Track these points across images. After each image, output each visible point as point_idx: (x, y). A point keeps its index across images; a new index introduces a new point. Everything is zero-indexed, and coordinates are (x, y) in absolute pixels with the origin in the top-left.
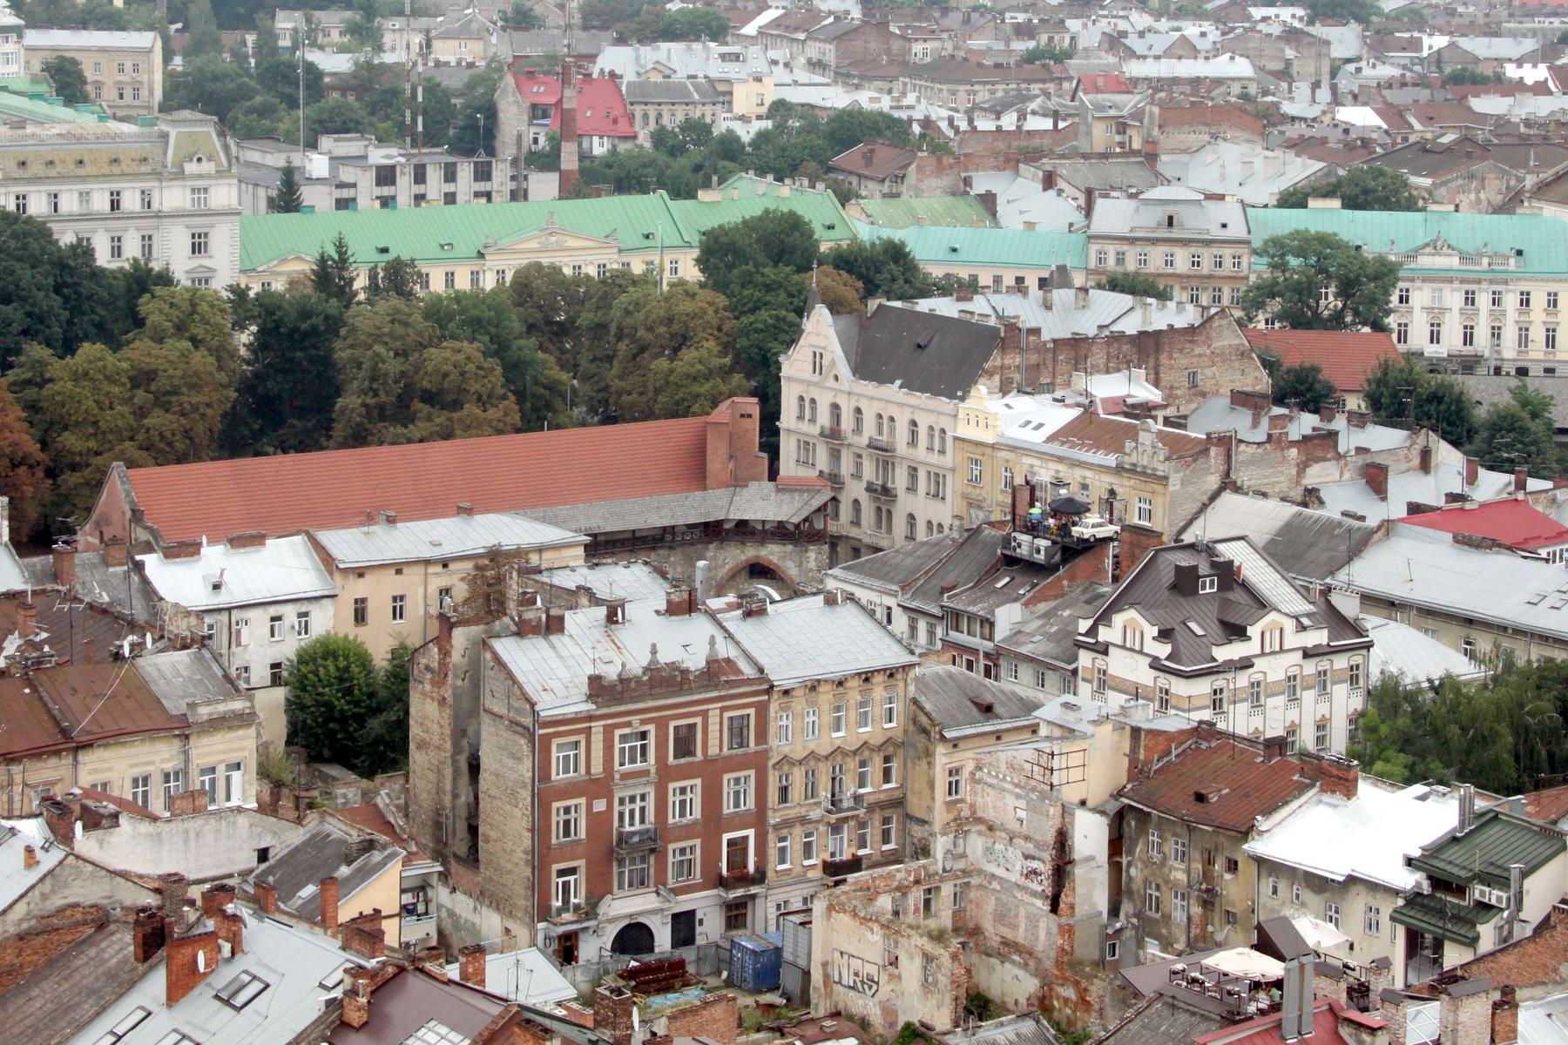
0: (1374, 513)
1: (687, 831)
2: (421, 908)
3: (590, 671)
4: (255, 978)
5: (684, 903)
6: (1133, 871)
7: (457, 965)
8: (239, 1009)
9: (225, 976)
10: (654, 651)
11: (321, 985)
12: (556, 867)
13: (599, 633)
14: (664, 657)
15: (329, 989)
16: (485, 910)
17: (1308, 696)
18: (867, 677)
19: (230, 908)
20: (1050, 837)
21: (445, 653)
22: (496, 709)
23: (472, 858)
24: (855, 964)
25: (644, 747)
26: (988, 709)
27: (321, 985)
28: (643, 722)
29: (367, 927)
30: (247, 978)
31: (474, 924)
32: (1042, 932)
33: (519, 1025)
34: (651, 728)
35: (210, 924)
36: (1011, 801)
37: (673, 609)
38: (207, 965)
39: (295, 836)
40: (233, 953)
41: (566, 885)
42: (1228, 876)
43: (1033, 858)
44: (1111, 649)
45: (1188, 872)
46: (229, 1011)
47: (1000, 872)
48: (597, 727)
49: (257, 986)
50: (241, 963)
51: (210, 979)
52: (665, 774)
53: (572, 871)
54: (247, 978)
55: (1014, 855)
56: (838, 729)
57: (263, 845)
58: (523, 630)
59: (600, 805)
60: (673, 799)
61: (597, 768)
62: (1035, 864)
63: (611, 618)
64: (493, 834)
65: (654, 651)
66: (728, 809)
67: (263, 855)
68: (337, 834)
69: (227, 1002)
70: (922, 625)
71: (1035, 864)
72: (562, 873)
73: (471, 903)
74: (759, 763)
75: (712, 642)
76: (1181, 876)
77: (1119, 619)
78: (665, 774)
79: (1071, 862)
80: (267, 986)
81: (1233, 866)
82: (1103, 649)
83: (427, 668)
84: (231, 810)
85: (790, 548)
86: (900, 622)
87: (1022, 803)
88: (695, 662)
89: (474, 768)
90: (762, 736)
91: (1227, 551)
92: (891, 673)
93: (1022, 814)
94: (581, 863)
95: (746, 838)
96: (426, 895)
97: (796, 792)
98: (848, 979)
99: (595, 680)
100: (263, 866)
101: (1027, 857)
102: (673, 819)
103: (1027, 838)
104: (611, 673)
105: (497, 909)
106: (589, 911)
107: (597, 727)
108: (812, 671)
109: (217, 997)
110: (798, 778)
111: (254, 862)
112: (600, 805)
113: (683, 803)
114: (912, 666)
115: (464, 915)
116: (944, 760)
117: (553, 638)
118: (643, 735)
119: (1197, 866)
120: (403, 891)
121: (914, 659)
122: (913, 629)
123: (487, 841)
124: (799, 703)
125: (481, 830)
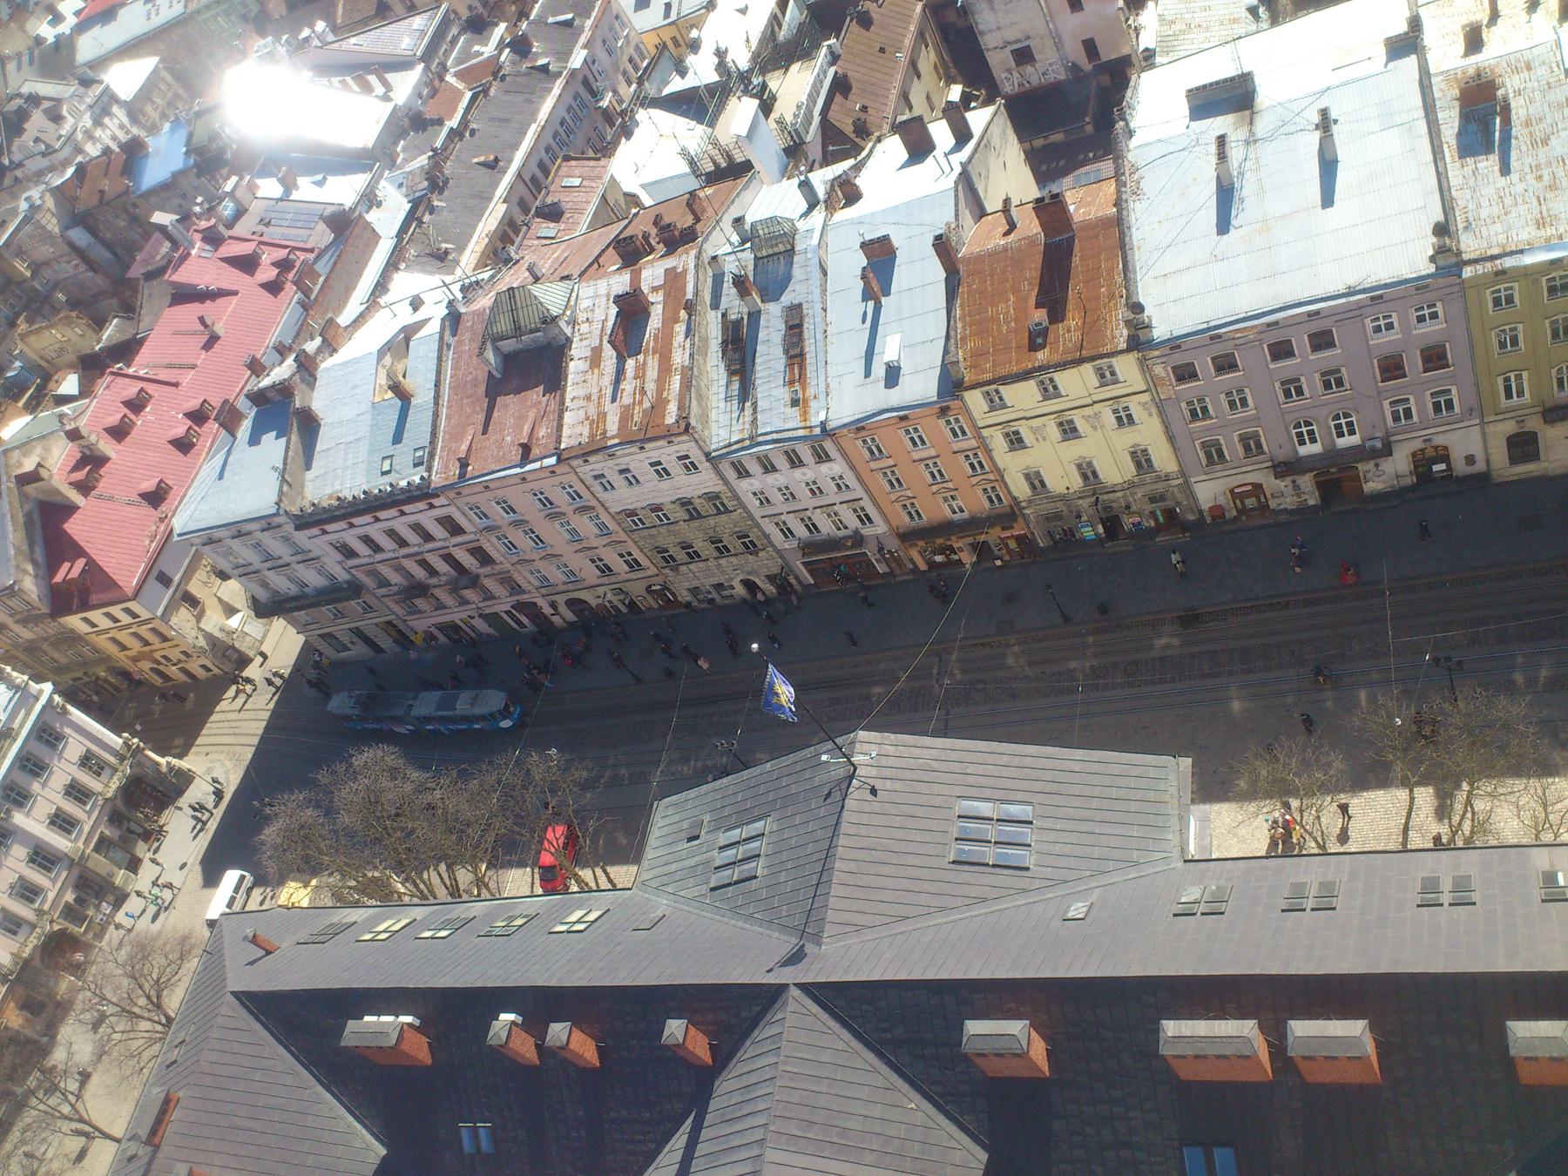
0: (65, 28)
6: (107, 236)
17: (106, 120)
20: (67, 249)
32: (101, 281)
42: (137, 210)
44: (24, 162)
45: (124, 220)
47: (66, 275)
55: (64, 265)
62: (75, 262)
71: (75, 262)
76: (122, 224)
77: (14, 148)
81: (135, 206)
82: (20, 165)
91: (25, 90)
93: (52, 250)
98: (54, 355)
103: (62, 256)
119: (124, 216)
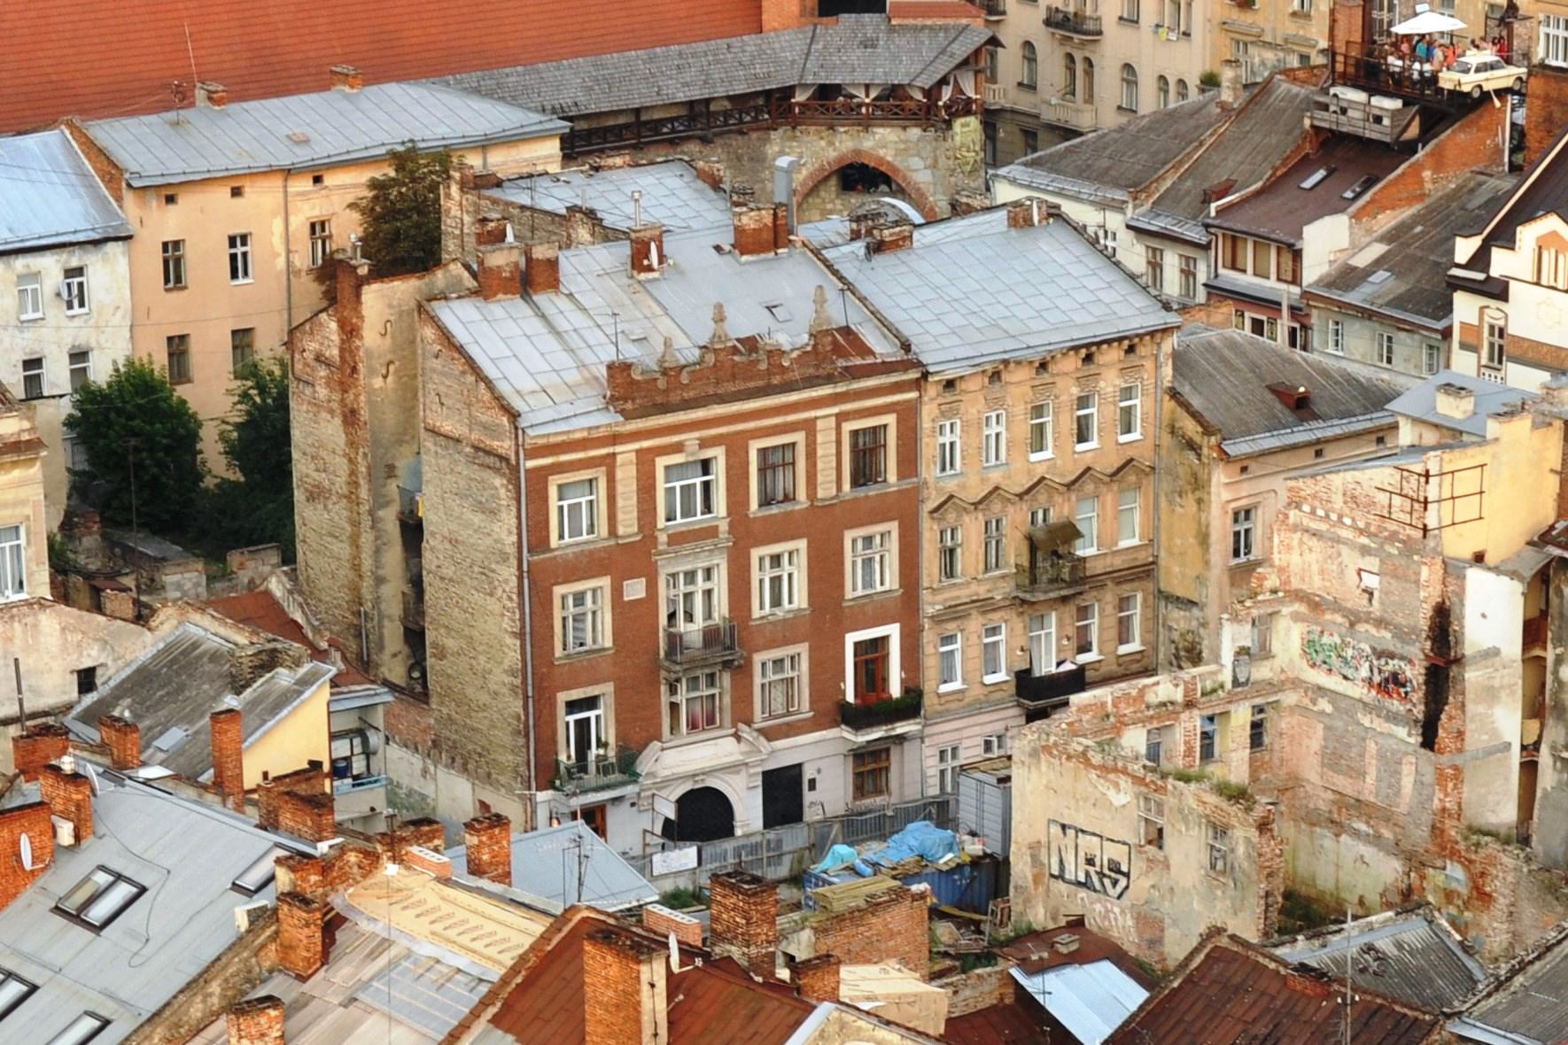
1: (785, 632)
2: (358, 766)
3: (609, 355)
4: (119, 877)
5: (786, 752)
7: (461, 850)
8: (98, 929)
9: (63, 880)
10: (720, 318)
11: (236, 887)
12: (563, 697)
13: (617, 287)
14: (741, 325)
15: (250, 893)
16: (442, 773)
18: (1088, 352)
19: (67, 764)
20: (1423, 618)
21: (350, 331)
22: (447, 427)
23: (417, 691)
24: (1089, 844)
25: (706, 486)
26: (1301, 407)
27: (236, 887)
28: (704, 444)
29: (302, 789)
30: (102, 879)
31: (424, 797)
33: (591, 937)
34: (718, 454)
35: (32, 791)
36: (1352, 560)
37: (746, 243)
38: (35, 860)
39: (142, 646)
40: (78, 838)
41: (583, 726)
43: (1392, 656)
46: (78, 931)
47: (1333, 682)
48: (626, 453)
49: (123, 891)
50: (96, 852)
51: (41, 881)
52: (745, 534)
53: (591, 703)
54: (102, 879)
56: (1128, 429)
57: (87, 663)
58: (485, 286)
59: (635, 590)
60: (760, 576)
61: (628, 525)
63: (639, 261)
64: (451, 643)
65: (720, 318)
66: (853, 588)
67: (86, 679)
68: (214, 643)
69: (77, 918)
70: (1171, 261)
72: (572, 706)
73: (417, 761)
74: (905, 511)
75: (820, 301)
77: (1528, 235)
78: (745, 534)
79: (1459, 661)
80: (143, 890)
83: (319, 358)
84: (28, 603)
85: (915, 132)
86: (1134, 255)
87: (1372, 563)
88: (790, 337)
89: (412, 531)
90: (909, 463)
92: (1130, 344)
93: (1371, 581)
94: (606, 690)
95: (884, 640)
96: (365, 742)
97: (969, 559)
99: (619, 370)
100: (90, 699)
101: (1380, 654)
102: (760, 609)
103: (1380, 623)
104: (644, 357)
105: (466, 770)
106: (627, 765)
107: (626, 453)
108: (995, 348)
109: (57, 910)
110: (971, 532)
111: (75, 695)
112: (635, 590)
113: (776, 581)
114: (1167, 331)
115: (405, 782)
116: (1226, 495)
117: (541, 299)
118: (706, 466)
120: (333, 737)
121: (1172, 319)
122: (1156, 266)
123: (441, 655)
124: (973, 401)
125: (430, 636)
